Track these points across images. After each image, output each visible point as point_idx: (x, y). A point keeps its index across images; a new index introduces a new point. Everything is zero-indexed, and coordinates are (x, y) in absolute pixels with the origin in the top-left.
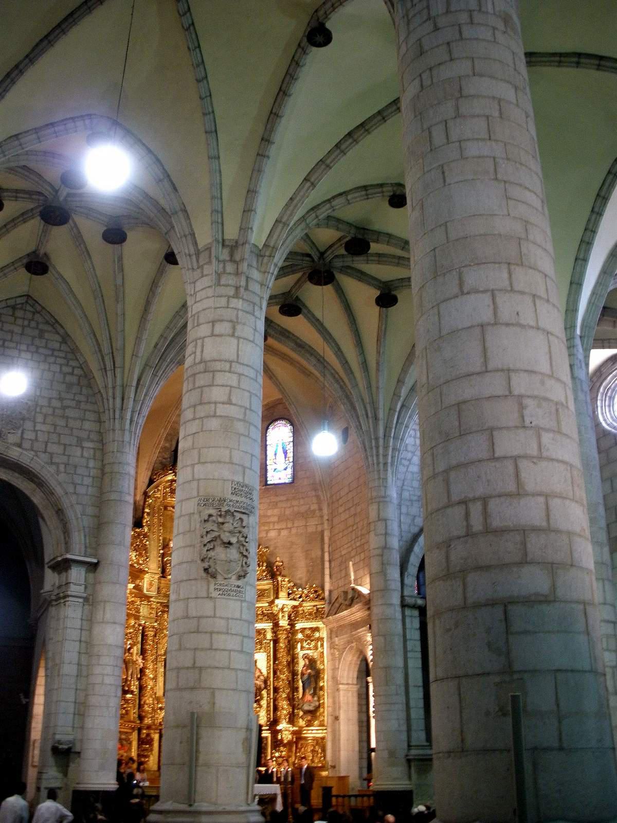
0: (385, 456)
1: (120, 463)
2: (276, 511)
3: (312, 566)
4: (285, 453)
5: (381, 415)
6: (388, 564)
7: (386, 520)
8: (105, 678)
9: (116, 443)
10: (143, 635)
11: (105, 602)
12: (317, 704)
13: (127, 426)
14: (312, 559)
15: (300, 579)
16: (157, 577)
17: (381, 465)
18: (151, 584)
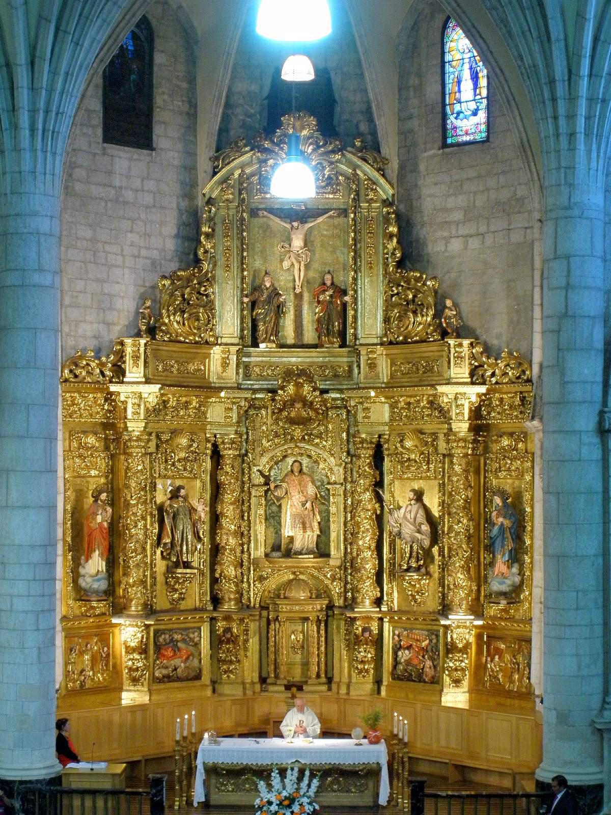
0: (571, 117)
1: (17, 215)
2: (461, 201)
3: (517, 311)
4: (475, 78)
5: (556, 29)
6: (568, 350)
7: (568, 257)
8: (15, 601)
9: (8, 177)
10: (216, 455)
11: (8, 471)
12: (517, 579)
13: (25, 142)
14: (516, 297)
15: (499, 336)
16: (234, 349)
17: (564, 142)
18: (225, 364)
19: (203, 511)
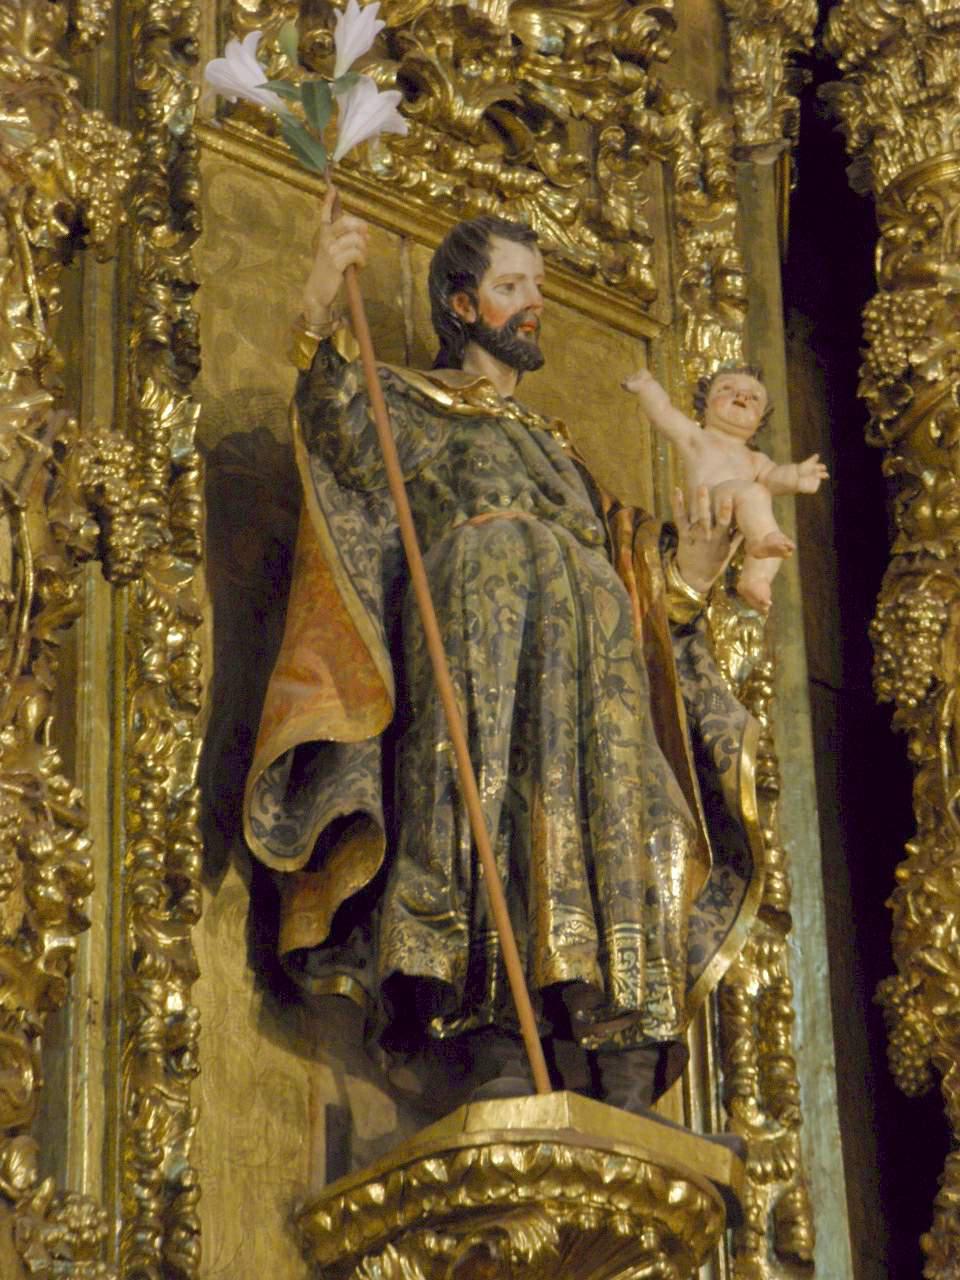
19: (746, 479)
